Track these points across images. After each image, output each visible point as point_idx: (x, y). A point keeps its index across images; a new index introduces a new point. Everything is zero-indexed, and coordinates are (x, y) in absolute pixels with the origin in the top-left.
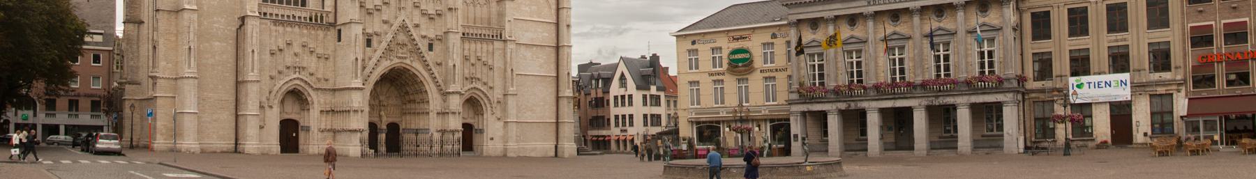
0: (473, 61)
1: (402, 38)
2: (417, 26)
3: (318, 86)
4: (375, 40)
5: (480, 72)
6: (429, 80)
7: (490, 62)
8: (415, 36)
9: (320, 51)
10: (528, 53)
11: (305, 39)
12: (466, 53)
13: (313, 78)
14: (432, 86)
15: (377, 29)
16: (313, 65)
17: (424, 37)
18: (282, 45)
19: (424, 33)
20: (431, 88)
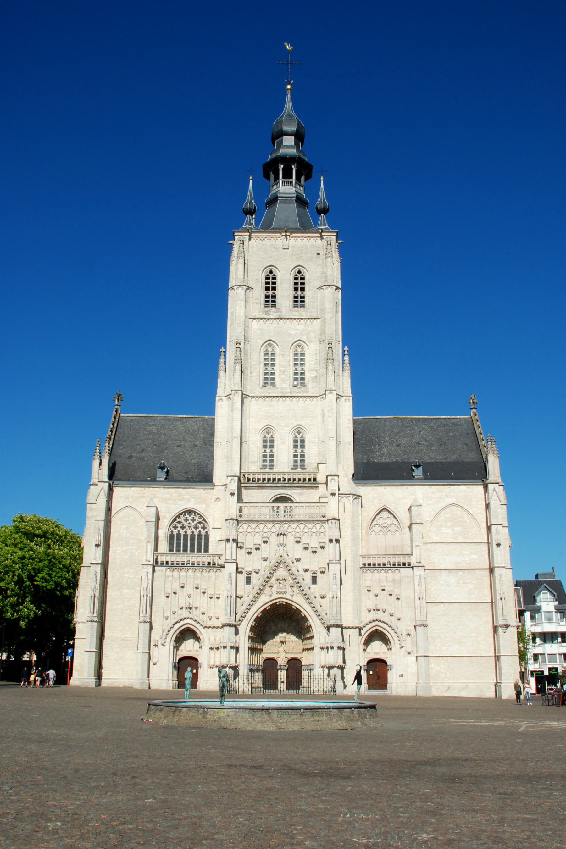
2: (298, 560)
3: (210, 623)
4: (254, 576)
5: (384, 602)
7: (396, 591)
8: (294, 570)
9: (210, 591)
10: (452, 578)
11: (198, 581)
12: (368, 583)
14: (316, 619)
16: (205, 605)
17: (306, 571)
20: (313, 621)
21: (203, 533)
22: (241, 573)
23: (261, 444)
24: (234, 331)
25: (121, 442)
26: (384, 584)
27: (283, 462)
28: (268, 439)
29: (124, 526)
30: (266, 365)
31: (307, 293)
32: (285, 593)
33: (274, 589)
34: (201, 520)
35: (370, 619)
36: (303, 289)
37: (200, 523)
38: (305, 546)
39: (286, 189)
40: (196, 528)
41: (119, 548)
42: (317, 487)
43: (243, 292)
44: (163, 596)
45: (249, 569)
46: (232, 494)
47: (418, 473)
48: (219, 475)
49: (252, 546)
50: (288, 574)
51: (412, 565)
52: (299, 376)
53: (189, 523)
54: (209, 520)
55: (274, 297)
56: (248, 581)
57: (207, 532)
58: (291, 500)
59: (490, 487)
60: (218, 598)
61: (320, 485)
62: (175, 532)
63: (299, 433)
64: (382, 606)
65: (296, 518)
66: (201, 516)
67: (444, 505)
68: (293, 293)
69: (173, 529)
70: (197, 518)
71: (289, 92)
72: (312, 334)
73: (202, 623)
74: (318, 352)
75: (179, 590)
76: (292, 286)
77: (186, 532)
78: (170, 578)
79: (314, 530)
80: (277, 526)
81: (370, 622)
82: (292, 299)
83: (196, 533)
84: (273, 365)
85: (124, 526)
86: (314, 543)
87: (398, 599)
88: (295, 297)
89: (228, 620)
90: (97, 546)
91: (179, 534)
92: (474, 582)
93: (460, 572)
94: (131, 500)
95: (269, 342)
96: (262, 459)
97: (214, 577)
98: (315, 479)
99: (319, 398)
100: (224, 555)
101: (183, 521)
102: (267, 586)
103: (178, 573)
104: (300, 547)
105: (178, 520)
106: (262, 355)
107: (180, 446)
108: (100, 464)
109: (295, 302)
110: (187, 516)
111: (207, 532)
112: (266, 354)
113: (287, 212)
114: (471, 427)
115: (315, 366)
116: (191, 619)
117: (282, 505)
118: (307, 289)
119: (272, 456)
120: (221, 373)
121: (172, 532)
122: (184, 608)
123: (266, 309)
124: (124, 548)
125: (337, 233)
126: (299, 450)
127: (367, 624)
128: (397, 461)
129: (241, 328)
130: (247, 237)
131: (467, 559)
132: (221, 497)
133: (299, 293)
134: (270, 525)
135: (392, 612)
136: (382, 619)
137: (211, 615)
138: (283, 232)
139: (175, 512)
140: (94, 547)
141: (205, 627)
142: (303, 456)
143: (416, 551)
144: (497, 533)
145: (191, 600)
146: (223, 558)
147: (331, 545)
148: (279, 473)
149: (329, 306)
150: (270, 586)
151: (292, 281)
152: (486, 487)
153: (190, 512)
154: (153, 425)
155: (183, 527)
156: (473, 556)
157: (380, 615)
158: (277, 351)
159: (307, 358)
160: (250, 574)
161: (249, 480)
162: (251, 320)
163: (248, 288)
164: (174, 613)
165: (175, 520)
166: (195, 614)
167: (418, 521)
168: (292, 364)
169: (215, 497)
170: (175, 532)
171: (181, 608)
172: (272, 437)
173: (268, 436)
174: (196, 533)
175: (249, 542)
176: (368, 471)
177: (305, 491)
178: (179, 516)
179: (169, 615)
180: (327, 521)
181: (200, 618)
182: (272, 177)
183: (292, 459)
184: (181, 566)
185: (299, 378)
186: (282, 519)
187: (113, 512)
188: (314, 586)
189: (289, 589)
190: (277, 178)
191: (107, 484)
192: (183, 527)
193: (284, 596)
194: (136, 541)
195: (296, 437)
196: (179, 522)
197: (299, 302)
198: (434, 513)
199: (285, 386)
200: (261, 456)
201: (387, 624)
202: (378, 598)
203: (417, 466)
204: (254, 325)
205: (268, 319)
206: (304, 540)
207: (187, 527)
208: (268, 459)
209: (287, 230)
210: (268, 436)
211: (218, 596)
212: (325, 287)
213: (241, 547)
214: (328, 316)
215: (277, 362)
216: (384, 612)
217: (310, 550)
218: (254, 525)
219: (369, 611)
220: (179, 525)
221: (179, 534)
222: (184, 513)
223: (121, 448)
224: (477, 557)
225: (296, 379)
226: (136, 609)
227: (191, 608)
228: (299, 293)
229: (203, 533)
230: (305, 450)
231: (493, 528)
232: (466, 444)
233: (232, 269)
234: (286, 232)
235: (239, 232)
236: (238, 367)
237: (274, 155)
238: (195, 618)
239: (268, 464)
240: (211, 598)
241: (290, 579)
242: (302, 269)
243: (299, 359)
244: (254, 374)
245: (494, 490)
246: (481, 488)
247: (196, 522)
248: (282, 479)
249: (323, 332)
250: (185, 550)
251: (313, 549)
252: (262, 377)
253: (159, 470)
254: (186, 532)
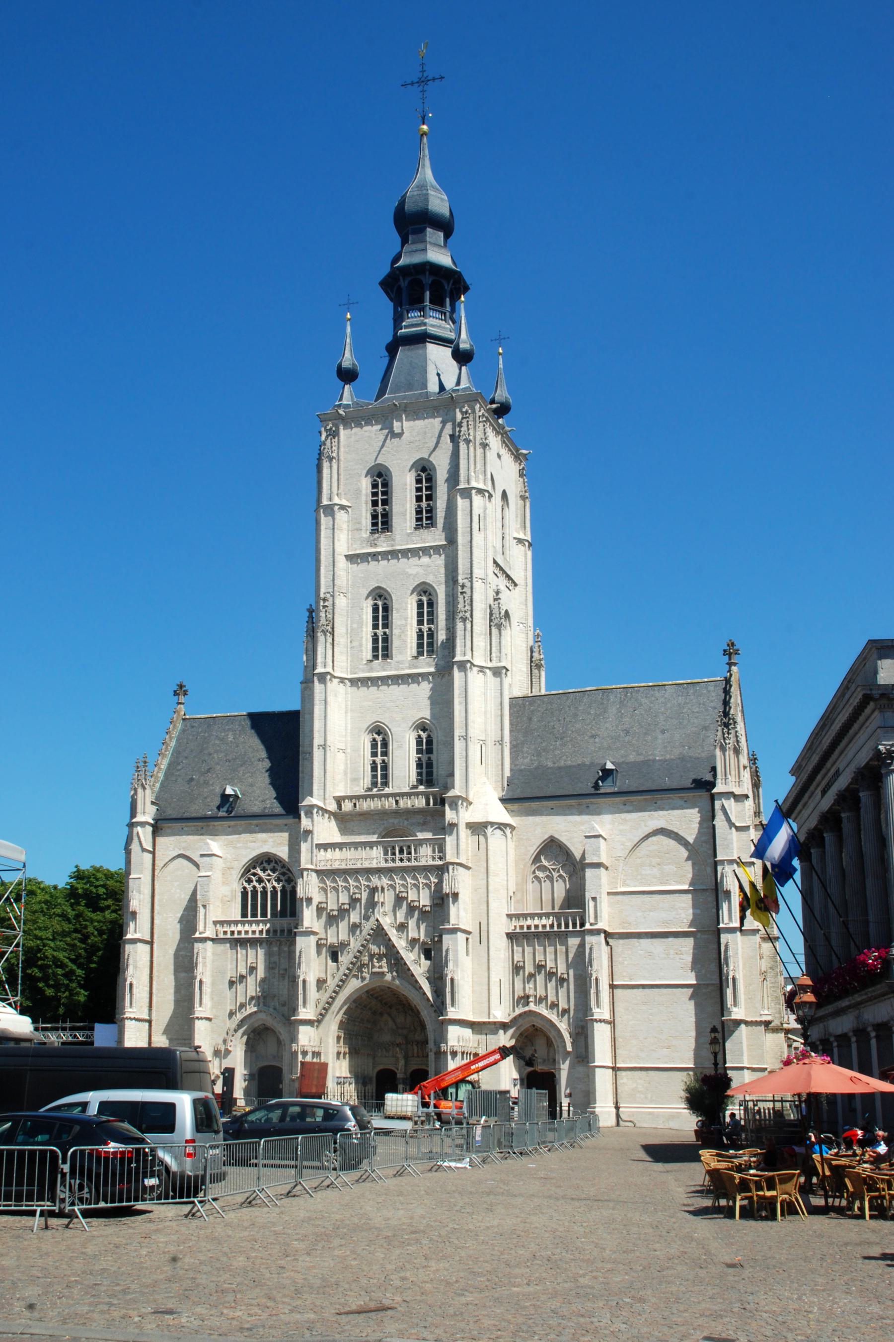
11: (275, 959)
16: (285, 992)
18: (243, 970)
34: (284, 870)
62: (249, 888)
69: (246, 885)
85: (176, 884)
119: (385, 767)
155: (260, 880)
167: (595, 860)
170: (249, 888)
192: (260, 880)
250: (254, 915)
254: (264, 888)
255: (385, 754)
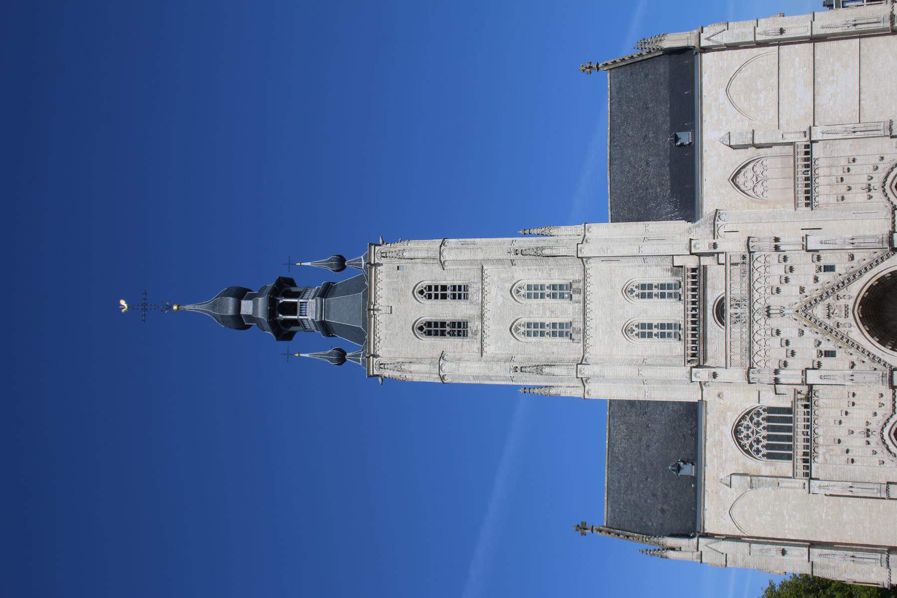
0: (842, 189)
1: (819, 311)
2: (802, 290)
4: (826, 346)
5: (858, 178)
6: (875, 270)
7: (844, 162)
9: (845, 406)
12: (833, 200)
13: (880, 412)
14: (882, 266)
15: (811, 344)
17: (816, 279)
19: (812, 279)
21: (765, 415)
22: (819, 364)
23: (647, 340)
24: (498, 374)
25: (643, 524)
26: (834, 178)
27: (672, 311)
28: (641, 330)
29: (757, 519)
30: (542, 334)
31: (449, 282)
32: (846, 307)
33: (842, 320)
34: (748, 418)
35: (882, 195)
36: (444, 288)
37: (751, 419)
38: (783, 281)
39: (310, 310)
40: (758, 424)
41: (787, 526)
42: (705, 267)
43: (447, 364)
44: (851, 466)
45: (814, 353)
46: (715, 375)
47: (685, 138)
48: (690, 395)
49: (784, 350)
50: (821, 303)
51: (808, 143)
52: (558, 292)
53: (753, 433)
54: (748, 406)
55: (453, 324)
56: (830, 354)
57: (764, 410)
58: (723, 299)
59: (704, 43)
60: (854, 395)
61: (702, 264)
62: (764, 451)
63: (632, 291)
64: (864, 180)
65: (745, 293)
66: (743, 418)
67: (727, 103)
68: (449, 302)
69: (761, 454)
70: (745, 423)
71: (182, 307)
72: (503, 276)
73: (888, 416)
74: (526, 268)
75: (844, 446)
76: (440, 302)
77: (764, 437)
78: (828, 457)
79: (762, 270)
80: (757, 317)
81: (886, 195)
82: (456, 302)
83: (765, 424)
84: (542, 325)
85: (757, 519)
86: (778, 270)
87: (854, 160)
88: (454, 298)
89: (884, 379)
90: (784, 552)
91: (767, 447)
92: (831, 60)
93: (818, 79)
94: (721, 509)
95: (513, 329)
96: (666, 339)
97: (825, 401)
98: (694, 270)
99: (587, 266)
100: (795, 387)
101: (749, 441)
102: (837, 330)
103: (820, 447)
104: (784, 288)
105: (748, 447)
106: (529, 339)
107: (648, 446)
108: (673, 549)
109: (460, 298)
110: (742, 436)
111: (764, 410)
112: (529, 334)
113: (341, 310)
114: (622, 70)
115: (545, 272)
116: (882, 429)
117: (729, 311)
118: (443, 283)
119: (662, 326)
120: (553, 391)
121: (763, 456)
122: (868, 439)
123: (470, 334)
124: (787, 518)
125: (371, 244)
126: (655, 291)
127: (889, 199)
128: (669, 165)
129: (494, 366)
130: (375, 360)
131: (800, 71)
132: (717, 392)
133: (449, 292)
134: (756, 327)
135: (871, 167)
136: (882, 179)
137: (877, 404)
138: (369, 313)
139: (738, 452)
140: (786, 557)
141: (894, 411)
142: (662, 286)
143: (789, 139)
144: (766, 33)
145: (856, 431)
146: (799, 388)
147: (782, 248)
148: (686, 316)
149: (466, 255)
150: (838, 326)
151: (433, 301)
152: (705, 50)
153: (736, 432)
154: (619, 482)
156: (797, 64)
157: (876, 183)
158: (524, 320)
159: (533, 282)
160: (821, 352)
161: (694, 355)
162: (484, 354)
163: (442, 357)
164: (875, 453)
165: (747, 452)
166: (875, 426)
167: (750, 136)
168: (541, 301)
169: (717, 399)
170: (764, 451)
171: (868, 443)
172: (637, 326)
173: (637, 330)
174: (765, 424)
175: (778, 353)
176: (684, 202)
177: (709, 283)
178: (742, 447)
179: (877, 460)
180: (750, 252)
181: (881, 419)
182: (293, 329)
183: (666, 300)
184: (810, 441)
185: (559, 291)
186: (747, 311)
187: (737, 533)
188: (837, 269)
189: (842, 302)
190: (296, 323)
191: (701, 540)
192: (758, 441)
193: (851, 307)
194: (777, 503)
195: (637, 296)
196: (751, 446)
197: (459, 293)
198: (739, 116)
199: (570, 311)
200: (662, 340)
201: (889, 174)
202: (852, 186)
203: (677, 139)
204: (489, 350)
205: (483, 331)
206: (776, 283)
207: (758, 436)
208: (666, 331)
209: (367, 309)
210: (637, 330)
211: (851, 395)
212: (442, 259)
213: (785, 364)
214: (480, 256)
215: (539, 320)
216: (872, 178)
217: (789, 275)
218: (756, 348)
219: (870, 197)
220: (755, 446)
221: (767, 447)
222: (738, 440)
223: (650, 524)
224: (797, 59)
225: (562, 296)
226: (870, 504)
227: (868, 430)
228: (449, 292)
229: (765, 415)
230: (655, 283)
231: (759, 38)
232: (646, 76)
233: (416, 378)
234: (370, 310)
235: (369, 370)
236: (547, 370)
237: (266, 326)
238: (881, 424)
239: (672, 331)
240: (853, 404)
241: (827, 301)
242: (418, 289)
243: (535, 292)
244: (555, 349)
245: (708, 39)
246: (705, 56)
247: (750, 423)
248: (694, 312)
249: (500, 261)
251: (788, 270)
252: (558, 339)
253: (682, 473)
255: (650, 326)
